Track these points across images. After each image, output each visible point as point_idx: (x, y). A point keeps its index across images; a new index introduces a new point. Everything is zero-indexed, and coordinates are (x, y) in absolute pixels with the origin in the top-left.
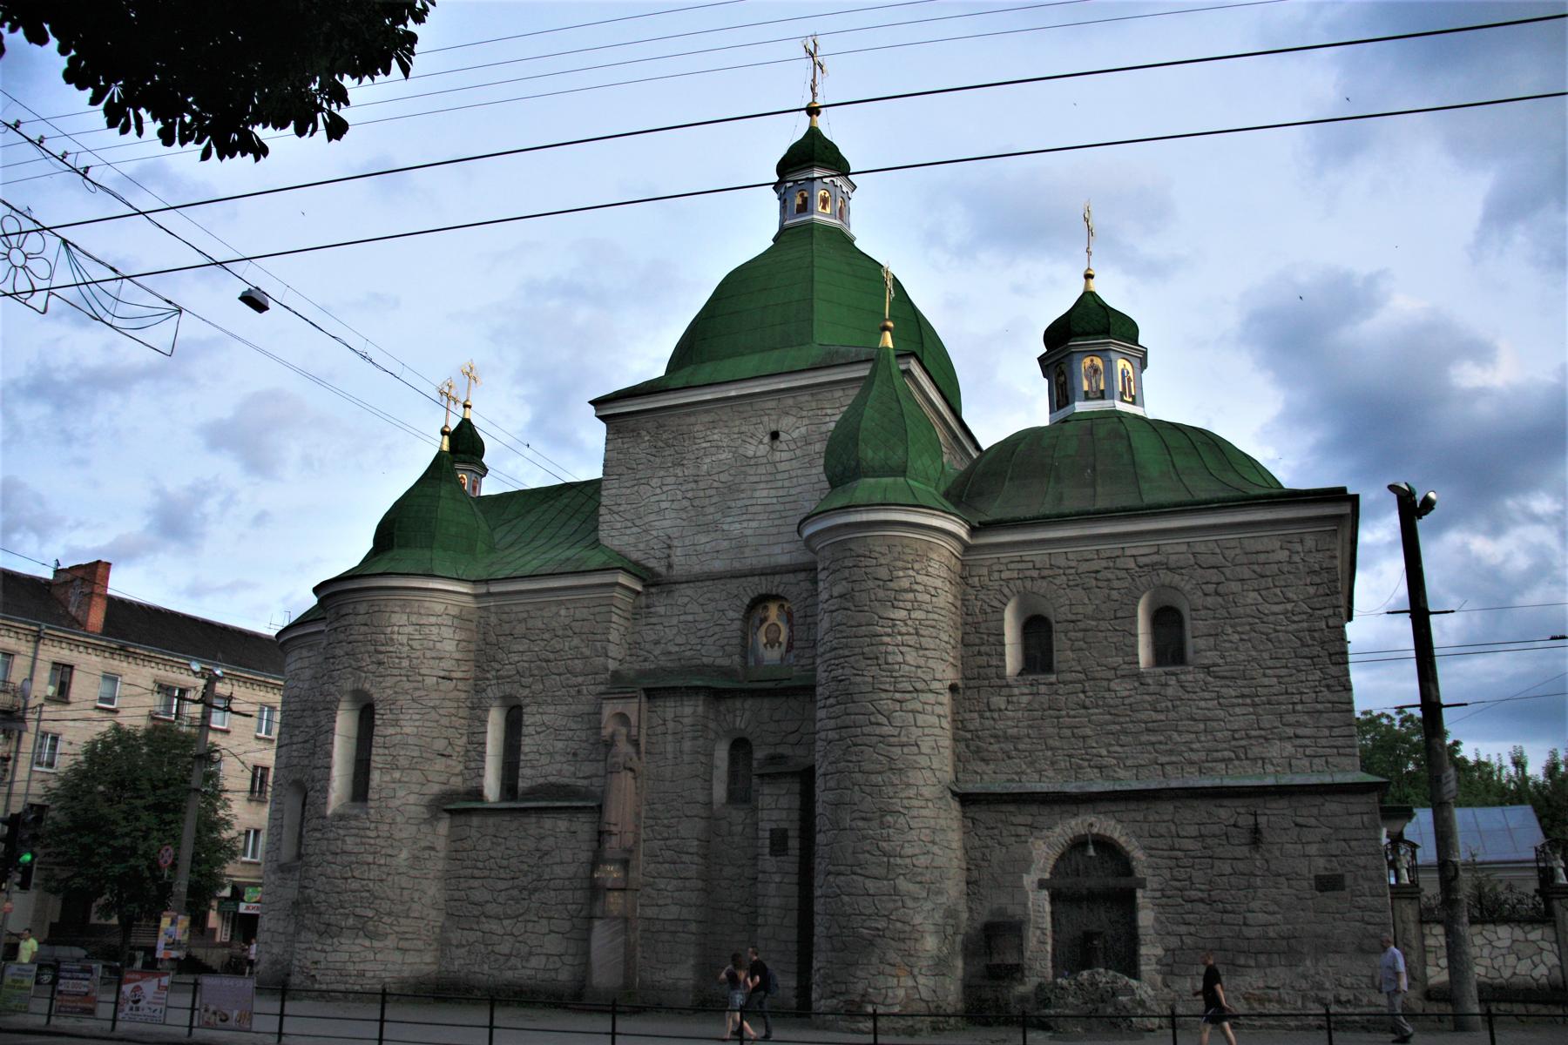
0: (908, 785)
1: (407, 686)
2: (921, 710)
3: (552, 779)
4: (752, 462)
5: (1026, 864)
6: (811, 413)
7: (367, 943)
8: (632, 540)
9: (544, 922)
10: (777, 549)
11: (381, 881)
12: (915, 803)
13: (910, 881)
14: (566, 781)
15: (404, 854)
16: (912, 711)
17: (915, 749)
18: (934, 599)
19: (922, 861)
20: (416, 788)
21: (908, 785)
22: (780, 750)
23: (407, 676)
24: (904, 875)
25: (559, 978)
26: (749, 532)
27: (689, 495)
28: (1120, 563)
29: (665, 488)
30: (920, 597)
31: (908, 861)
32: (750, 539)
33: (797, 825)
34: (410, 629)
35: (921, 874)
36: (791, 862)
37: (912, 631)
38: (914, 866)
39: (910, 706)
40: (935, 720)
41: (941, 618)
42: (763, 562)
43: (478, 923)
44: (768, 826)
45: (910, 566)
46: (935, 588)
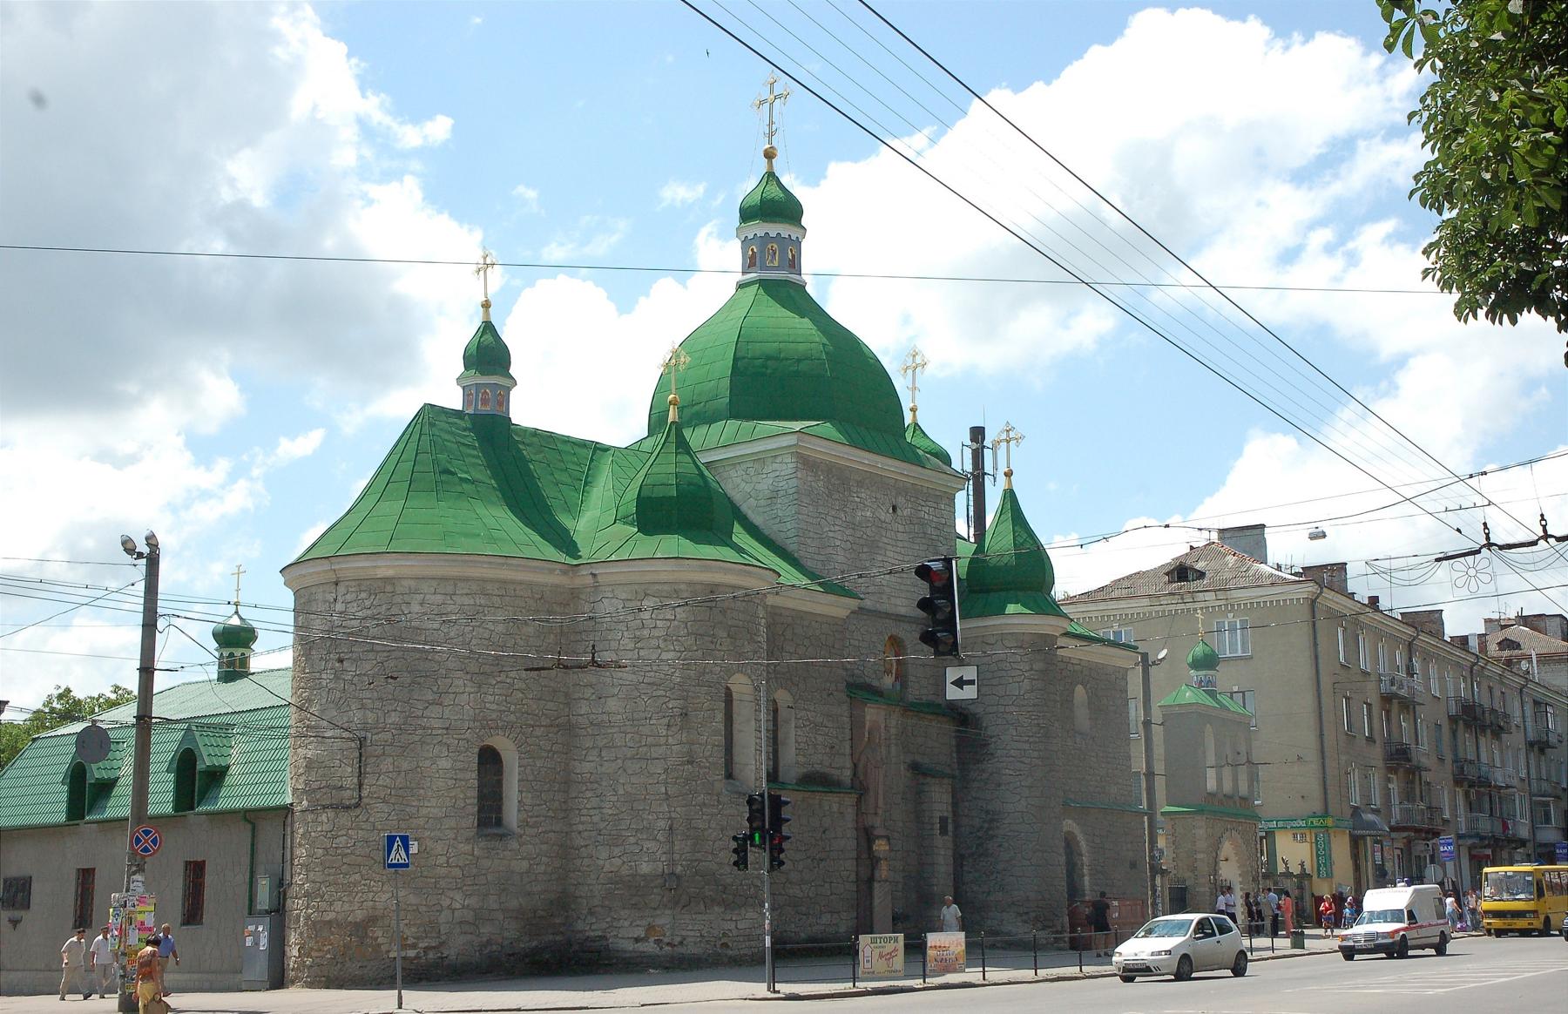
3: (818, 767)
4: (884, 525)
6: (912, 499)
8: (820, 566)
9: (827, 885)
10: (898, 602)
14: (827, 770)
22: (919, 759)
25: (841, 930)
26: (884, 583)
27: (850, 538)
28: (1070, 667)
29: (837, 528)
32: (885, 588)
33: (950, 815)
36: (949, 838)
42: (892, 610)
43: (783, 889)
44: (938, 814)
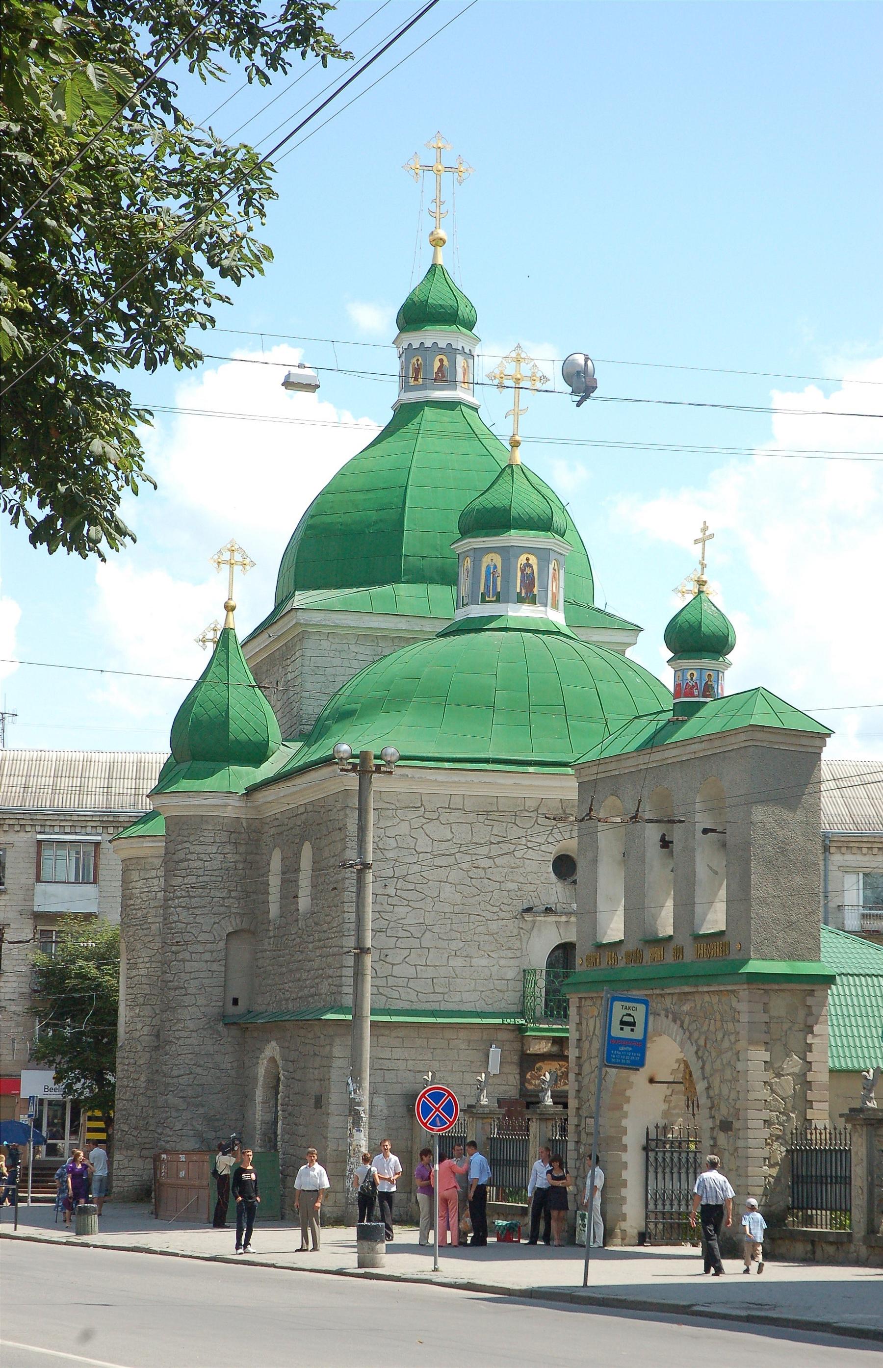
0: (179, 1020)
1: (141, 933)
2: (188, 958)
5: (256, 1079)
7: (125, 1153)
11: (131, 1100)
12: (182, 1034)
13: (175, 1096)
15: (143, 1079)
16: (183, 961)
17: (183, 991)
18: (206, 864)
19: (184, 1080)
20: (148, 1021)
21: (179, 1020)
23: (140, 925)
24: (172, 1091)
30: (193, 864)
31: (175, 1080)
34: (139, 884)
35: (183, 1091)
37: (184, 893)
38: (180, 1084)
39: (180, 956)
40: (204, 964)
41: (214, 878)
45: (186, 839)
46: (209, 854)
